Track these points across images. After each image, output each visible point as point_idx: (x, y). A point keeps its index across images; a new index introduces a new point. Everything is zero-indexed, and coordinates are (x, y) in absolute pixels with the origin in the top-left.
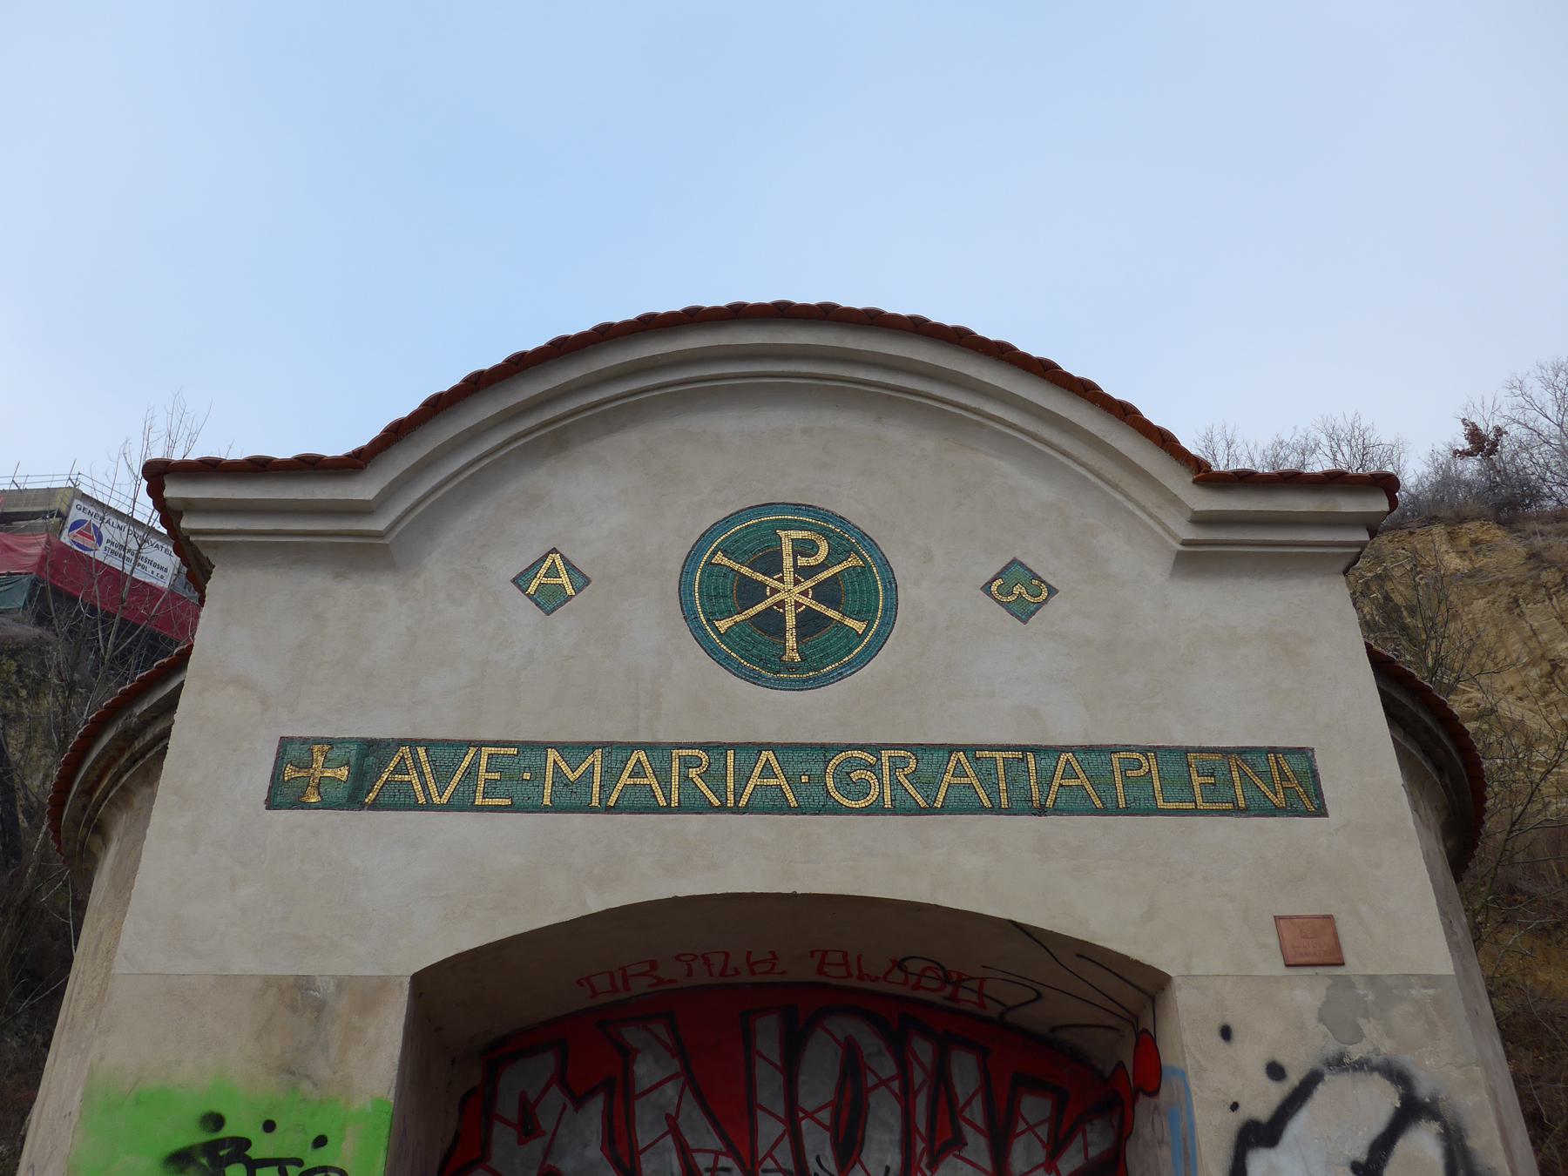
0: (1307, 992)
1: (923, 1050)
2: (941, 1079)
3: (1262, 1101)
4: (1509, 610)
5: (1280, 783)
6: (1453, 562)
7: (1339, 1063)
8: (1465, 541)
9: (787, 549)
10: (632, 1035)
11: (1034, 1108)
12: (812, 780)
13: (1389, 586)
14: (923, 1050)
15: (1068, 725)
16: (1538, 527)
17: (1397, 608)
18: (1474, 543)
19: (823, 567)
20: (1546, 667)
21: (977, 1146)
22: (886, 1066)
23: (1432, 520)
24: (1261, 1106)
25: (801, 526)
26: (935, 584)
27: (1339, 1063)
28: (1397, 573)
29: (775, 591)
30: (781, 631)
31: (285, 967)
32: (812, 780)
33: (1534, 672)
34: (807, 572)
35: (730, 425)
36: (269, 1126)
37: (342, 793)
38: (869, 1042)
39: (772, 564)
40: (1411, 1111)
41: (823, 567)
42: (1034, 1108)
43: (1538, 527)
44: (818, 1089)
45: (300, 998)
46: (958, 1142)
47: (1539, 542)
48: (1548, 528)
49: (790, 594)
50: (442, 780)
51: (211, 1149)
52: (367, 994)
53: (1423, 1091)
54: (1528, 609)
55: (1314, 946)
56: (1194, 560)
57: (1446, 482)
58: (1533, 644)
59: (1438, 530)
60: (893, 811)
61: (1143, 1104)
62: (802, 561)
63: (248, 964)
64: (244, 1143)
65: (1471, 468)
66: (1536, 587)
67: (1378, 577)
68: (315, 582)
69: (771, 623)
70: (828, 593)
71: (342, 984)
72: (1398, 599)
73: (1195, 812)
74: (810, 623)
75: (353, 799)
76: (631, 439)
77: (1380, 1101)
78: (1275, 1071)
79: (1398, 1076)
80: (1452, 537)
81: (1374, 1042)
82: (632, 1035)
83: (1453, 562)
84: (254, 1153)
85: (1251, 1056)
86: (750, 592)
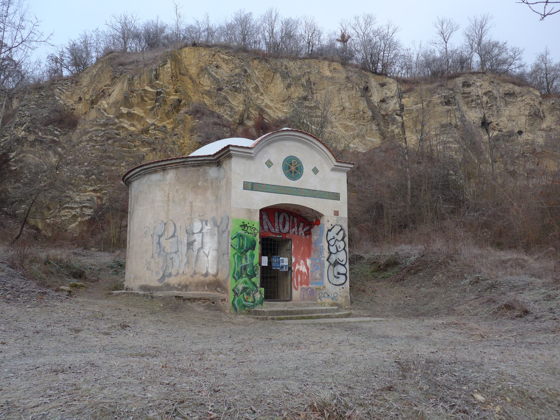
0: (335, 218)
1: (292, 217)
2: (293, 220)
4: (338, 91)
5: (336, 196)
6: (328, 73)
7: (337, 225)
8: (332, 68)
11: (302, 224)
13: (310, 75)
14: (292, 217)
15: (318, 188)
16: (351, 69)
18: (334, 69)
20: (342, 108)
21: (296, 228)
22: (288, 218)
23: (325, 59)
26: (307, 169)
27: (337, 225)
28: (313, 72)
31: (248, 208)
33: (339, 109)
34: (295, 166)
35: (287, 143)
37: (250, 188)
38: (286, 216)
39: (291, 164)
40: (341, 229)
42: (302, 224)
43: (351, 69)
44: (281, 220)
45: (249, 211)
46: (294, 227)
47: (350, 74)
48: (353, 70)
49: (293, 168)
52: (256, 211)
54: (342, 92)
55: (336, 213)
56: (333, 170)
57: (331, 46)
58: (340, 101)
59: (327, 63)
61: (316, 226)
63: (244, 207)
65: (339, 45)
66: (346, 87)
67: (308, 72)
68: (244, 160)
69: (291, 172)
70: (297, 169)
71: (253, 210)
72: (312, 80)
74: (295, 172)
75: (252, 190)
76: (276, 144)
77: (340, 228)
79: (341, 226)
80: (329, 66)
81: (340, 223)
83: (328, 73)
86: (289, 168)
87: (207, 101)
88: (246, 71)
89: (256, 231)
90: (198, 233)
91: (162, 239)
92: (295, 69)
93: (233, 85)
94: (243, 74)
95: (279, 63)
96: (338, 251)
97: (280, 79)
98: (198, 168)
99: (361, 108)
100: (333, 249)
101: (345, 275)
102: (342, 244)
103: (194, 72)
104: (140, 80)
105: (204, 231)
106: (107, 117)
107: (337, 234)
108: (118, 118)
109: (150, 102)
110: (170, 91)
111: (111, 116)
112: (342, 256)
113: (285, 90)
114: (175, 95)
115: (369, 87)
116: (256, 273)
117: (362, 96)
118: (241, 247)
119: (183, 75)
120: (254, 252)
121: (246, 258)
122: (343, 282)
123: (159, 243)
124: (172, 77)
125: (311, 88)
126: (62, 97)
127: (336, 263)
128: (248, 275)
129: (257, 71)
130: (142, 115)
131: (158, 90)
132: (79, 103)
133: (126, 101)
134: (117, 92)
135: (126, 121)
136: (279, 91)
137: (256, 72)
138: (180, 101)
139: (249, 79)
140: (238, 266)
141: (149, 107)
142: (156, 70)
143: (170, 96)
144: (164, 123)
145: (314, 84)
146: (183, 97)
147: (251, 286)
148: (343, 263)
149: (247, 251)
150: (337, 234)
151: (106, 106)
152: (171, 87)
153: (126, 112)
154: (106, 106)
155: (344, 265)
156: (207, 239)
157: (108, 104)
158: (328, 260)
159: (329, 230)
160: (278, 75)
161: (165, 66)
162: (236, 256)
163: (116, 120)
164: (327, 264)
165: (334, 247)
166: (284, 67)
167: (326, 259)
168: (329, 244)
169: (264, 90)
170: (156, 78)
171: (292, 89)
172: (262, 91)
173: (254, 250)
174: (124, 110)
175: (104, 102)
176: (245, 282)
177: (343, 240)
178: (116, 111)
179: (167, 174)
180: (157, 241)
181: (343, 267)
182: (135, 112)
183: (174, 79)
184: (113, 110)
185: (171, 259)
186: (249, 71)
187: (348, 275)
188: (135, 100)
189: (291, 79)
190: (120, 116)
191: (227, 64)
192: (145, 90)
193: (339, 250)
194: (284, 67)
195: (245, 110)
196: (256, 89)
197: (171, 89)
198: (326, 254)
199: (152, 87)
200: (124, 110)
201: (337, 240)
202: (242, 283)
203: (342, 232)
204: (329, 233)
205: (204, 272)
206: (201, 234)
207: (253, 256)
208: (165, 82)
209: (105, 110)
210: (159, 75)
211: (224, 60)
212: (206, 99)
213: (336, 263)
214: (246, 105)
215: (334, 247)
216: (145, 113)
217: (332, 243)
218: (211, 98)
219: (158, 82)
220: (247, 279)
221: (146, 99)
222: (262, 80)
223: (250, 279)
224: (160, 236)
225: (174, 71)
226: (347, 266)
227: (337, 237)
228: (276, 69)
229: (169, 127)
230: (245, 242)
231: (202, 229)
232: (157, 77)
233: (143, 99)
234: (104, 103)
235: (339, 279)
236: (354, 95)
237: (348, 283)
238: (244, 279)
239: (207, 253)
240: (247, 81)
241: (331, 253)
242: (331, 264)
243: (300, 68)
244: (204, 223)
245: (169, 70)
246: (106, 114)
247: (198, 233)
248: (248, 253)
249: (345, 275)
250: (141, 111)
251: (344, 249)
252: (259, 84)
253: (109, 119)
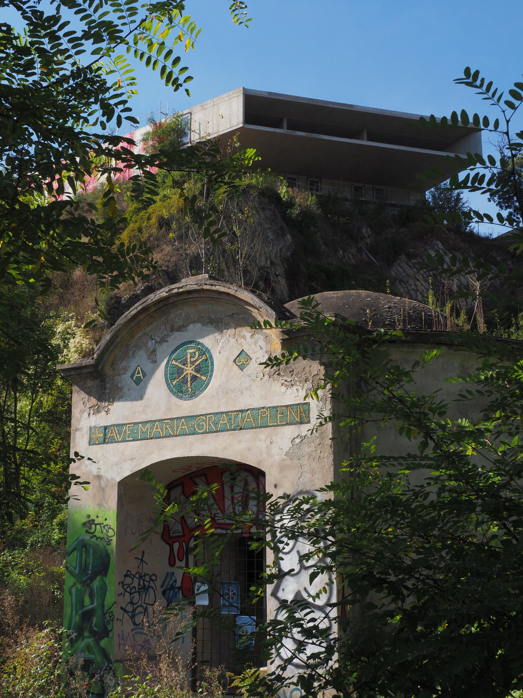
9: (189, 356)
10: (198, 480)
12: (192, 425)
19: (197, 360)
29: (186, 370)
32: (192, 425)
34: (192, 363)
36: (97, 517)
37: (102, 440)
41: (197, 360)
49: (189, 370)
50: (120, 434)
51: (89, 521)
60: (208, 433)
62: (192, 360)
64: (94, 520)
70: (198, 370)
73: (278, 426)
82: (198, 480)
84: (96, 522)
89: (111, 533)
116: (109, 628)
118: (84, 569)
120: (107, 580)
121: (91, 596)
128: (93, 633)
140: (77, 612)
147: (99, 658)
149: (92, 579)
162: (74, 590)
173: (105, 575)
176: (88, 648)
202: (82, 651)
207: (104, 589)
220: (90, 641)
223: (97, 642)
230: (91, 560)
238: (86, 641)
248: (96, 584)
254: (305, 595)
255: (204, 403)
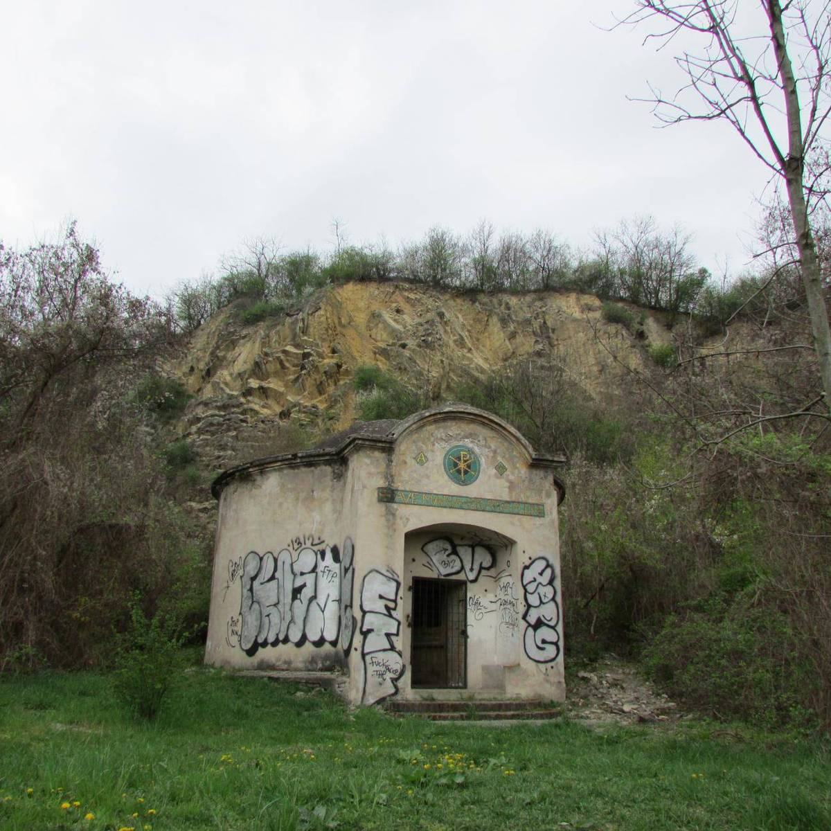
3: (528, 562)
17: (547, 328)
24: (527, 563)
25: (462, 450)
30: (460, 473)
34: (465, 461)
39: (459, 458)
40: (548, 566)
49: (462, 466)
53: (550, 563)
67: (543, 312)
69: (459, 471)
70: (469, 466)
72: (549, 324)
78: (530, 558)
79: (547, 561)
85: (527, 556)
86: (456, 465)
87: (383, 365)
88: (443, 314)
90: (310, 573)
91: (256, 583)
92: (521, 308)
93: (423, 338)
94: (438, 319)
95: (495, 301)
96: (541, 602)
97: (499, 325)
98: (313, 468)
99: (632, 367)
100: (533, 600)
101: (556, 644)
102: (549, 591)
103: (362, 320)
104: (279, 335)
105: (319, 570)
106: (228, 394)
107: (541, 574)
108: (244, 395)
109: (294, 369)
110: (324, 352)
111: (235, 393)
112: (549, 612)
113: (507, 342)
114: (332, 357)
115: (646, 331)
117: (633, 347)
119: (344, 326)
122: (553, 655)
123: (251, 590)
124: (327, 330)
125: (548, 337)
126: (165, 367)
127: (539, 624)
129: (458, 314)
130: (282, 389)
131: (306, 351)
132: (191, 375)
133: (257, 369)
134: (245, 354)
135: (256, 400)
136: (498, 344)
137: (460, 316)
138: (339, 366)
139: (448, 329)
141: (292, 377)
142: (303, 320)
143: (323, 358)
144: (314, 402)
145: (553, 330)
146: (345, 359)
148: (552, 623)
150: (541, 574)
151: (228, 378)
152: (326, 344)
153: (257, 386)
154: (228, 378)
155: (553, 628)
156: (324, 582)
157: (231, 375)
158: (524, 618)
159: (527, 567)
160: (495, 319)
161: (317, 314)
163: (242, 400)
164: (523, 624)
165: (536, 595)
166: (503, 306)
167: (520, 616)
168: (526, 591)
169: (473, 344)
170: (303, 332)
171: (519, 339)
172: (470, 345)
174: (254, 383)
175: (225, 373)
177: (551, 582)
178: (242, 385)
179: (268, 479)
180: (248, 587)
181: (552, 631)
182: (271, 386)
183: (330, 332)
184: (239, 383)
185: (268, 616)
186: (447, 315)
187: (561, 644)
188: (271, 367)
189: (516, 324)
190: (248, 392)
191: (413, 306)
192: (285, 352)
193: (544, 601)
194: (503, 306)
195: (442, 377)
196: (461, 343)
197: (325, 350)
198: (521, 609)
199: (297, 346)
200: (254, 383)
201: (540, 583)
203: (549, 571)
204: (526, 571)
205: (316, 638)
206: (314, 574)
208: (317, 337)
209: (226, 384)
210: (307, 327)
211: (408, 300)
212: (381, 361)
213: (539, 624)
214: (444, 368)
215: (536, 595)
216: (286, 386)
217: (531, 588)
218: (388, 360)
219: (306, 338)
221: (287, 365)
222: (469, 328)
224: (253, 579)
225: (329, 320)
226: (560, 628)
227: (540, 579)
228: (491, 311)
229: (322, 407)
231: (316, 567)
232: (305, 331)
233: (283, 367)
234: (224, 375)
235: (545, 652)
236: (619, 345)
237: (561, 658)
239: (323, 606)
240: (446, 331)
241: (529, 606)
242: (530, 625)
243: (529, 307)
244: (319, 556)
245: (323, 319)
246: (228, 391)
247: (310, 573)
249: (556, 644)
250: (280, 383)
251: (553, 599)
252: (465, 334)
253: (231, 397)
254: (543, 619)
255: (472, 490)
